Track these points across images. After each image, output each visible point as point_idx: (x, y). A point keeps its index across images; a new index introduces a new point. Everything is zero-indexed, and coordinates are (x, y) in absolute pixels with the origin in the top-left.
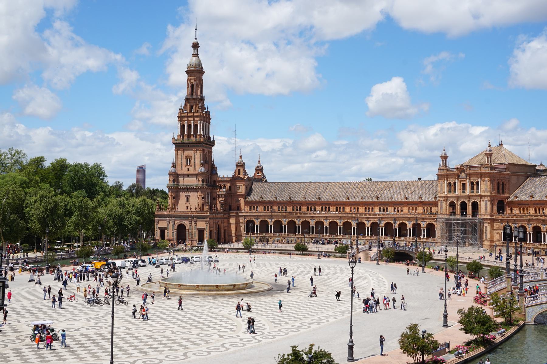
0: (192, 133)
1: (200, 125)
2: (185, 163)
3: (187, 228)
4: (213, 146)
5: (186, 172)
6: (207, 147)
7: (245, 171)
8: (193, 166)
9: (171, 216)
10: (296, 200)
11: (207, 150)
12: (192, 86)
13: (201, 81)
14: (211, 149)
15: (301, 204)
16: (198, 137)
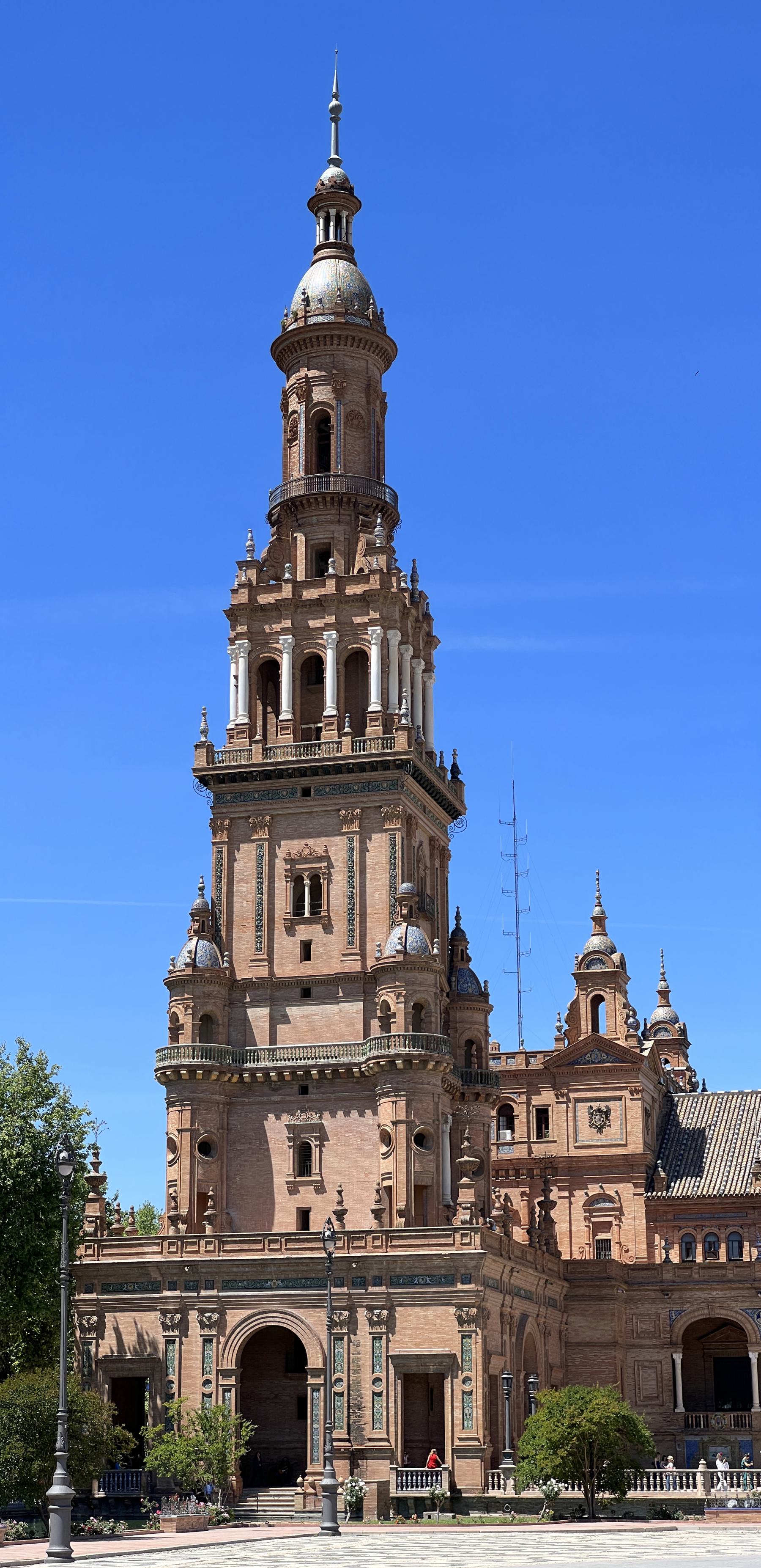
0: (330, 709)
2: (283, 905)
3: (314, 1360)
8: (340, 926)
16: (373, 730)
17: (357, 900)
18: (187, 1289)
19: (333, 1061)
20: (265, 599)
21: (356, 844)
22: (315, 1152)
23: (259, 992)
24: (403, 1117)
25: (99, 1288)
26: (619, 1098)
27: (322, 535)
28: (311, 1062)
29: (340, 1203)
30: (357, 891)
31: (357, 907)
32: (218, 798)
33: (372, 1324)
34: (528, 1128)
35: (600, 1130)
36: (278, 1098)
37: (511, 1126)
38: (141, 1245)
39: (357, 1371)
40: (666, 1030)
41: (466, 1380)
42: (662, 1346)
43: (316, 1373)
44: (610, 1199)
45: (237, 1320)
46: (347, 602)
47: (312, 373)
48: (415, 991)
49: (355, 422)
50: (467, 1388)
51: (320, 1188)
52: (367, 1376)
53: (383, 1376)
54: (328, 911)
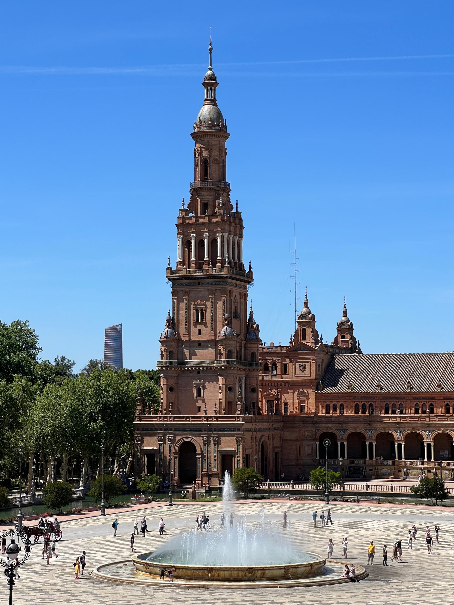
0: (206, 258)
1: (222, 242)
2: (193, 319)
3: (198, 451)
4: (249, 282)
5: (195, 337)
6: (237, 286)
7: (315, 333)
9: (166, 427)
10: (422, 390)
11: (236, 292)
12: (205, 163)
13: (223, 152)
14: (246, 288)
15: (433, 398)
16: (219, 265)
17: (213, 317)
18: (165, 430)
19: (206, 365)
20: (188, 221)
21: (213, 301)
22: (202, 391)
23: (186, 344)
24: (224, 383)
25: (141, 430)
26: (308, 362)
27: (205, 200)
28: (200, 365)
29: (206, 408)
30: (213, 315)
31: (214, 320)
32: (174, 285)
33: (214, 441)
34: (281, 370)
35: (303, 371)
36: (192, 375)
37: (276, 369)
38: (152, 418)
39: (210, 454)
40: (344, 325)
41: (238, 457)
42: (313, 440)
43: (199, 454)
44: (305, 393)
45: (178, 439)
46: (211, 224)
47: (202, 146)
48: (228, 347)
49: (216, 162)
50: (238, 459)
51: (203, 401)
52: (212, 455)
53: (216, 455)
54: (206, 320)
